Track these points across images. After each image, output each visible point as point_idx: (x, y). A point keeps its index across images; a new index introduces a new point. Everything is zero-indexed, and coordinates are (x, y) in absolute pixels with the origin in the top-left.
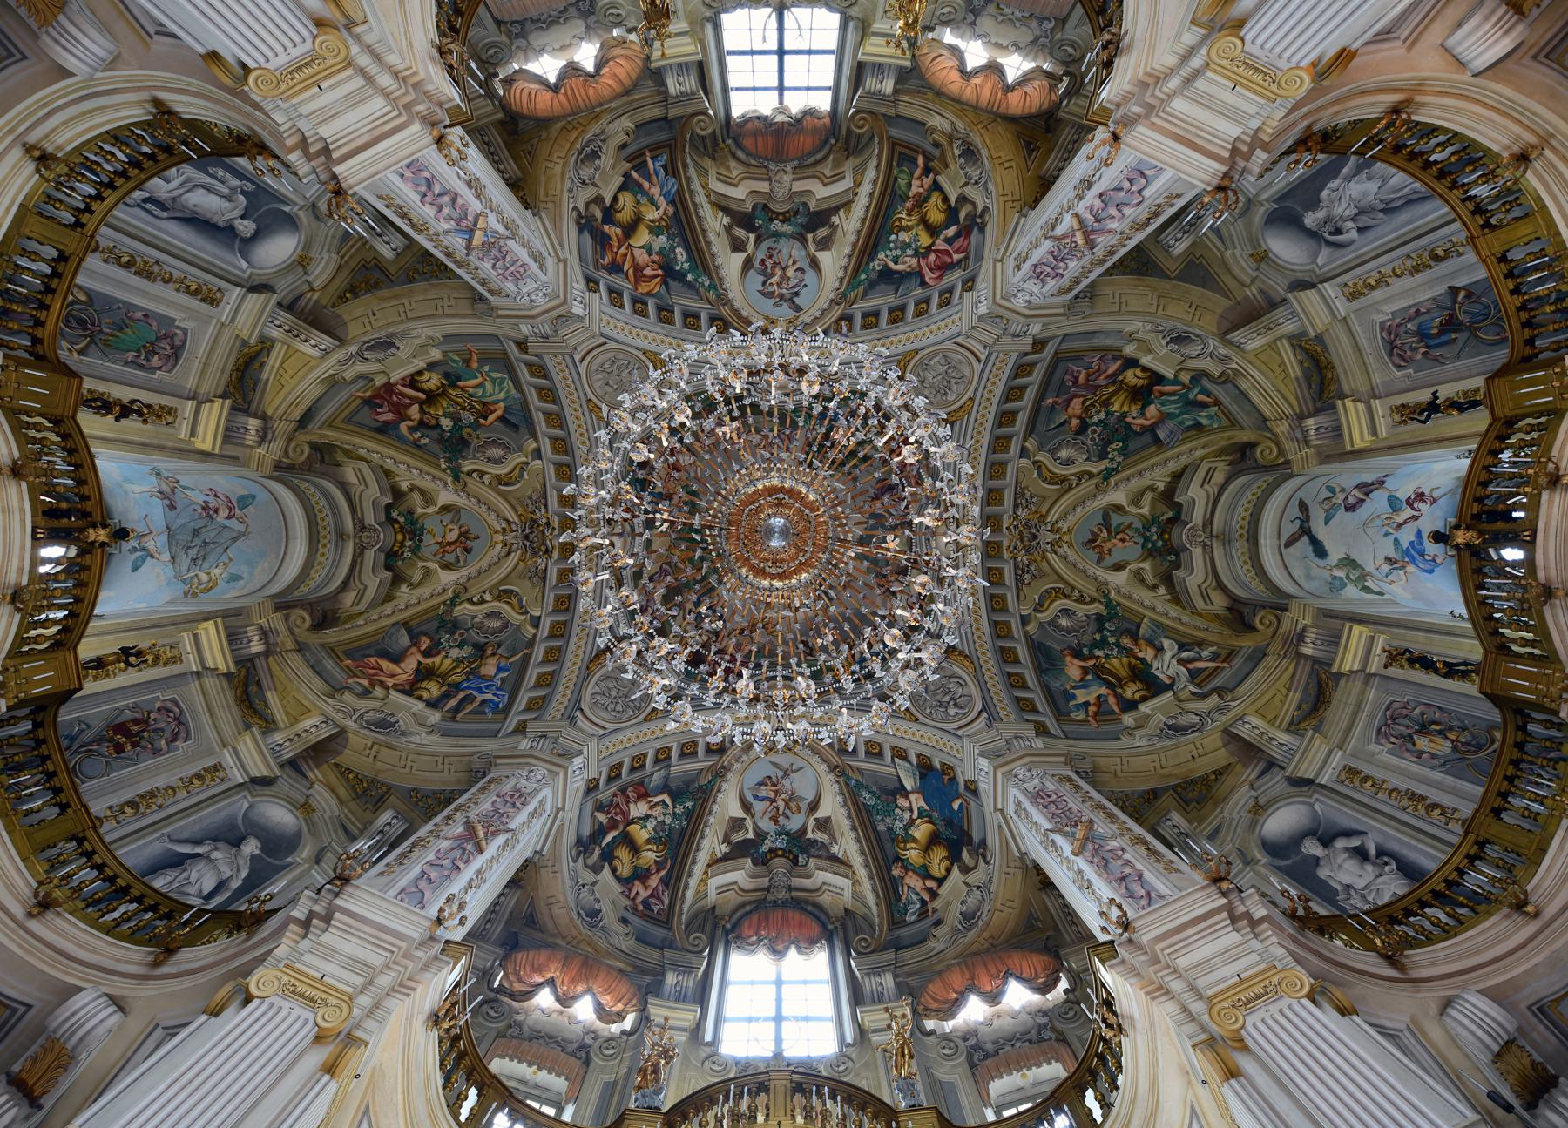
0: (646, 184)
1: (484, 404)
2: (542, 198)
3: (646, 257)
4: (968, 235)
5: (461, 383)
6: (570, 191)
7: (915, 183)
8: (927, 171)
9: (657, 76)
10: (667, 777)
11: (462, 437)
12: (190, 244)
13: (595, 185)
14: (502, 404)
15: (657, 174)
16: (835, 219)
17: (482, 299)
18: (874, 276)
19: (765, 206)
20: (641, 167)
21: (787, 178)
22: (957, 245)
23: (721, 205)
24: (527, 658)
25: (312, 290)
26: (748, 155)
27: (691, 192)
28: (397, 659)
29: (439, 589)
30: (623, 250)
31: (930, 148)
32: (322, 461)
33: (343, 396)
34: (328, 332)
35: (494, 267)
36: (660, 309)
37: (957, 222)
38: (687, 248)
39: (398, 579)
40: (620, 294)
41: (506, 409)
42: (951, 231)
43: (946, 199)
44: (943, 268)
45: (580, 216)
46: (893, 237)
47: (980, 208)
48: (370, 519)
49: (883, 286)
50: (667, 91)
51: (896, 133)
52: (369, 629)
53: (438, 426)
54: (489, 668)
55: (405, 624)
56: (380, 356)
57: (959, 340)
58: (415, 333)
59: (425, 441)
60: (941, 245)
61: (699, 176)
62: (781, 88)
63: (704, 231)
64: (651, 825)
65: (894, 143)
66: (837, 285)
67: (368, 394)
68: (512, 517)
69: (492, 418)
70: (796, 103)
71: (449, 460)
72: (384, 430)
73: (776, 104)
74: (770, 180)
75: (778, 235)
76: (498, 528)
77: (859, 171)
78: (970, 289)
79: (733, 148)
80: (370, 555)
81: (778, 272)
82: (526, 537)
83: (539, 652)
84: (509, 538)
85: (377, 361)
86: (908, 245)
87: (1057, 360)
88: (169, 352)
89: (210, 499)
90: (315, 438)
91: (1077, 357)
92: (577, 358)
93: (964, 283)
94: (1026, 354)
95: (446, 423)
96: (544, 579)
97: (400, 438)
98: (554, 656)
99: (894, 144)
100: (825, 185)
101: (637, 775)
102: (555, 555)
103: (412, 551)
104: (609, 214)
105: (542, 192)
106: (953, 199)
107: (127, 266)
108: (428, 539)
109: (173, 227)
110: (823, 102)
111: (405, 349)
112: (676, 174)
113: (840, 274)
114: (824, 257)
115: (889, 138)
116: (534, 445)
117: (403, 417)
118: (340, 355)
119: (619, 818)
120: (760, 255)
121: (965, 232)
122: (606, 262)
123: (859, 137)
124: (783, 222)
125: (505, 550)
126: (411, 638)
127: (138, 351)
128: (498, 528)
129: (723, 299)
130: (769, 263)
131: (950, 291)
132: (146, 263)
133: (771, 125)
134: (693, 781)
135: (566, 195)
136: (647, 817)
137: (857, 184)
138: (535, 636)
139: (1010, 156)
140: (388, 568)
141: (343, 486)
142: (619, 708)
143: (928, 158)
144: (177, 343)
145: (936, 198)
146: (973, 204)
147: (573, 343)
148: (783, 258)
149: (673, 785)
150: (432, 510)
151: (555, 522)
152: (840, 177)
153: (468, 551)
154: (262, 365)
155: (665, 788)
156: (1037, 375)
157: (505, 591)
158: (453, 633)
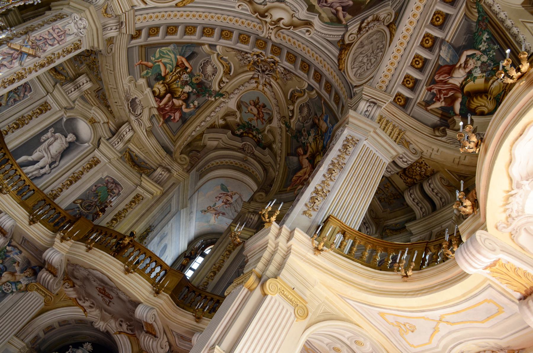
1: (177, 66)
5: (163, 74)
10: (451, 45)
11: (197, 84)
12: (71, 159)
14: (178, 57)
24: (326, 103)
25: (108, 123)
28: (300, 167)
29: (279, 130)
32: (199, 152)
33: (160, 131)
34: (123, 123)
35: (52, 45)
39: (269, 146)
41: (183, 56)
48: (240, 145)
52: (281, 172)
53: (188, 93)
54: (324, 126)
55: (288, 155)
56: (140, 107)
58: (126, 87)
59: (196, 103)
64: (477, 73)
67: (162, 119)
68: (250, 74)
69: (187, 64)
71: (210, 95)
72: (184, 119)
76: (255, 85)
80: (257, 153)
82: (263, 71)
83: (324, 94)
84: (262, 81)
85: (143, 108)
88: (114, 185)
89: (221, 200)
90: (179, 151)
92: (143, 6)
95: (187, 89)
96: (289, 72)
97: (191, 114)
98: (329, 87)
101: (429, 69)
102: (277, 59)
103: (258, 134)
107: (71, 183)
108: (254, 123)
109: (62, 162)
111: (135, 94)
116: (206, 46)
117: (179, 108)
118: (135, 125)
119: (451, 94)
125: (268, 86)
126: (295, 155)
127: (109, 195)
128: (255, 85)
132: (72, 177)
134: (469, 26)
136: (470, 74)
138: (317, 92)
140: (264, 148)
141: (217, 148)
142: (373, 61)
144: (112, 181)
147: (128, 8)
149: (462, 43)
150: (238, 114)
151: (258, 51)
153: (264, 106)
154: (136, 156)
155: (458, 51)
157: (291, 97)
158: (302, 135)
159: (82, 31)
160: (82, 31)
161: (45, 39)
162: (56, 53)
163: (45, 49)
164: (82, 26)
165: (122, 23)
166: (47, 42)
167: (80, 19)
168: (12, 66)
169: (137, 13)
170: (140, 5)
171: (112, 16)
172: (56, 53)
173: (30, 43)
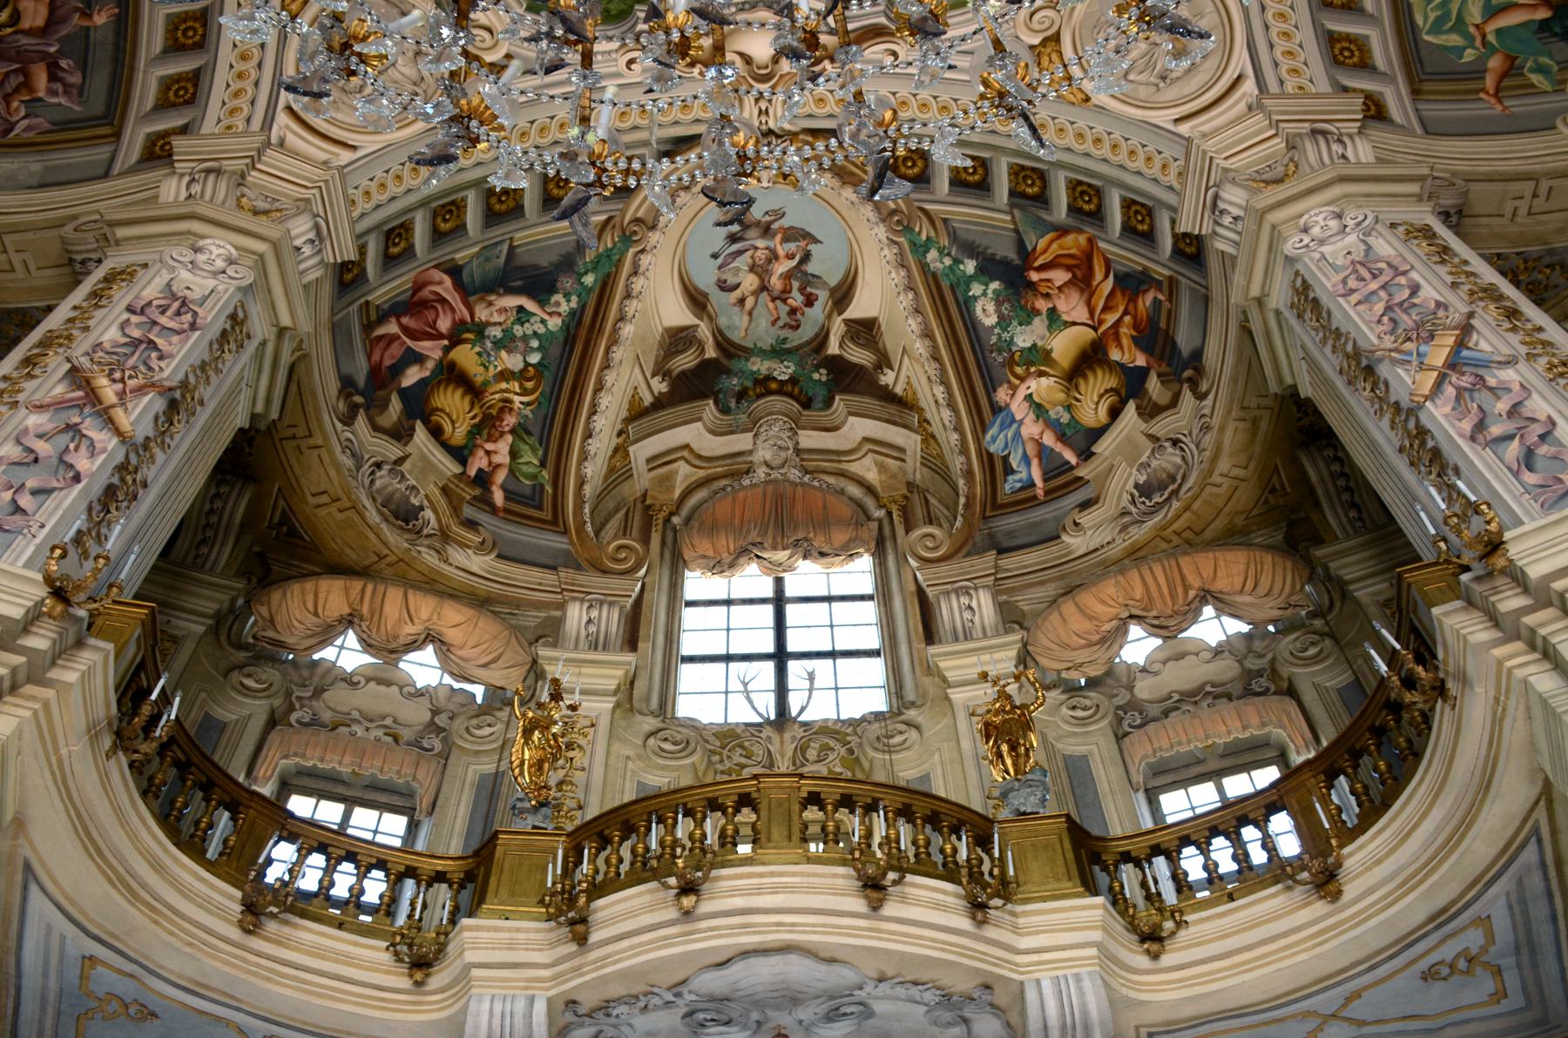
0: (1049, 440)
2: (1266, 414)
3: (1062, 305)
4: (375, 371)
6: (1206, 428)
7: (503, 457)
8: (483, 480)
9: (1011, 617)
13: (1154, 438)
15: (1026, 460)
16: (660, 386)
17: (1445, 216)
18: (567, 282)
19: (806, 404)
20: (1056, 470)
21: (764, 453)
22: (396, 351)
23: (899, 406)
26: (842, 492)
27: (958, 428)
30: (1111, 319)
31: (483, 518)
36: (1042, 199)
37: (404, 394)
38: (972, 325)
40: (1128, 229)
42: (412, 376)
43: (436, 432)
44: (416, 304)
45: (1194, 384)
46: (534, 359)
47: (361, 422)
49: (543, 262)
50: (995, 596)
51: (553, 541)
57: (346, 156)
60: (432, 350)
61: (941, 456)
62: (779, 601)
63: (936, 357)
65: (556, 522)
66: (645, 260)
70: (752, 580)
73: (788, 578)
74: (798, 451)
75: (779, 352)
77: (619, 467)
78: (344, 267)
79: (870, 503)
81: (776, 283)
86: (498, 344)
87: (111, 119)
91: (67, 131)
92: (1249, 86)
93: (362, 277)
94: (184, 130)
99: (555, 522)
100: (687, 447)
104: (1132, 385)
105: (1264, 425)
106: (421, 434)
110: (697, 584)
112: (988, 459)
113: (638, 284)
114: (676, 313)
115: (566, 532)
120: (817, 313)
121: (382, 379)
122: (1149, 298)
123: (625, 530)
124: (769, 378)
129: (898, 222)
130: (797, 299)
131: (389, 261)
133: (796, 544)
135: (1216, 422)
137: (620, 451)
139: (322, 512)
143: (485, 502)
145: (458, 433)
146: (376, 428)
147: (1258, 120)
148: (766, 310)
152: (655, 461)
156: (148, 81)
159: (1351, 223)
160: (1351, 223)
161: (1389, 308)
162: (1449, 279)
163: (1433, 305)
164: (1334, 224)
165: (1314, 132)
166: (1401, 304)
167: (1306, 230)
168: (1516, 387)
169: (1273, 87)
170: (1245, 94)
171: (1292, 160)
172: (1449, 279)
173: (1408, 346)
